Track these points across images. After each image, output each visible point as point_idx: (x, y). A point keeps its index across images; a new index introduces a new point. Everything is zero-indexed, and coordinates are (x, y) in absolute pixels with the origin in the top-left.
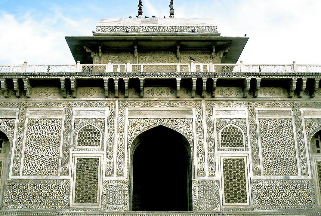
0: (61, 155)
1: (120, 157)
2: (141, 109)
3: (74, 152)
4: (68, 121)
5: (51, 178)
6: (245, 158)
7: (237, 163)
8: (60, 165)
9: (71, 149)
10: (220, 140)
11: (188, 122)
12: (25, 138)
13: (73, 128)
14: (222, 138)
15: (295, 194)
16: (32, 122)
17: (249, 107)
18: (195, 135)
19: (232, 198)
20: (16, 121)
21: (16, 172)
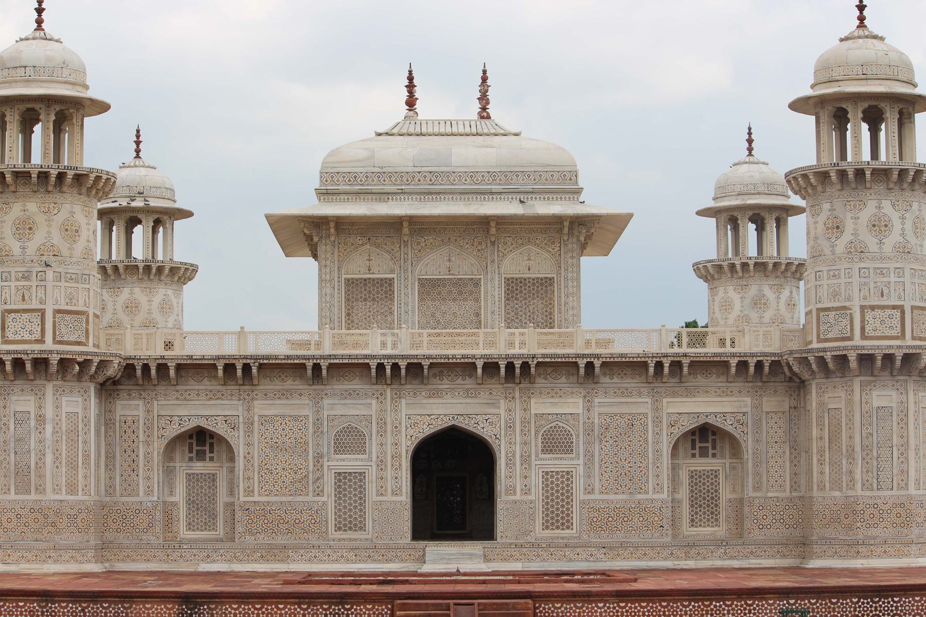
0: (311, 468)
1: (396, 469)
2: (425, 401)
3: (329, 463)
4: (318, 420)
5: (300, 499)
6: (574, 470)
7: (563, 476)
8: (311, 482)
9: (325, 459)
10: (540, 445)
11: (493, 419)
12: (256, 445)
13: (325, 430)
14: (542, 443)
15: (641, 519)
16: (265, 420)
17: (585, 397)
18: (503, 438)
19: (552, 524)
20: (241, 419)
21: (249, 492)
